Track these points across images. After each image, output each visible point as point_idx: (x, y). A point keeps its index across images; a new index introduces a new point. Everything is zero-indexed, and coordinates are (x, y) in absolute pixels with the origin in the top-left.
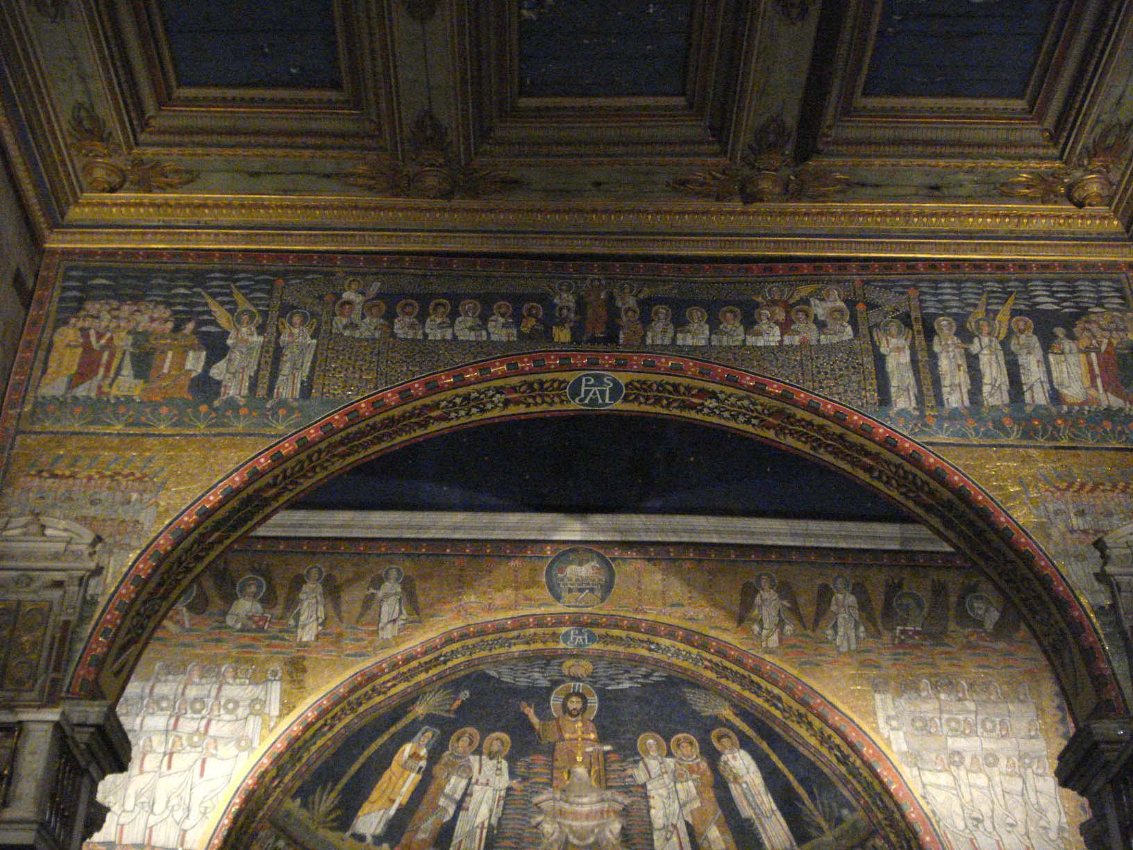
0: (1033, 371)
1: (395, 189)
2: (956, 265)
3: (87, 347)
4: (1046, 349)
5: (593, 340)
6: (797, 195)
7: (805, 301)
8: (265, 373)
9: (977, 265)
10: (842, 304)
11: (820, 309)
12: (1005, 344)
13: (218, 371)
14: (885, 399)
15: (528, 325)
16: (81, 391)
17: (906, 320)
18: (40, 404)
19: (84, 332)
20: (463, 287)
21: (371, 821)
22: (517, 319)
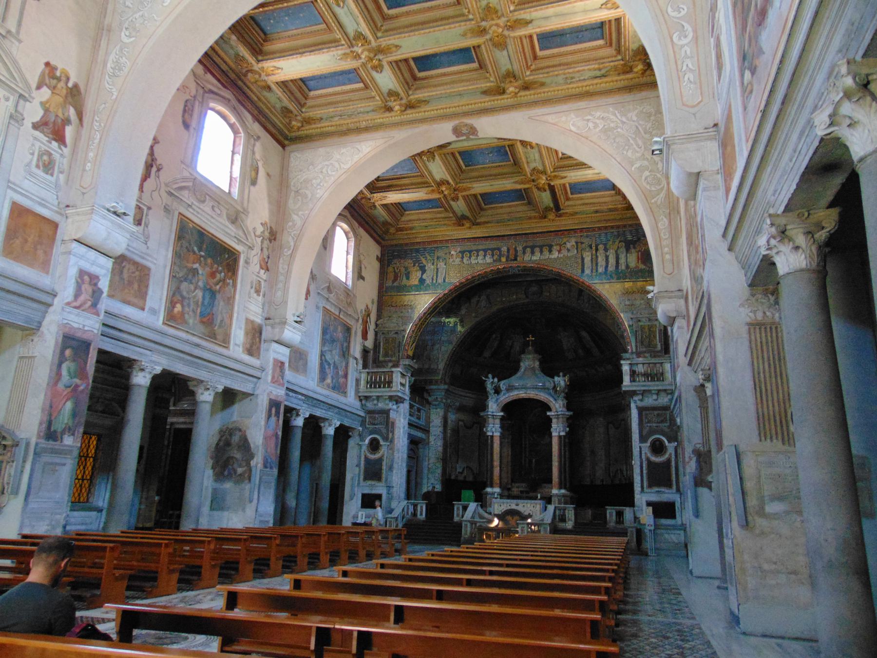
0: (622, 261)
1: (460, 225)
2: (606, 228)
3: (395, 271)
4: (627, 253)
5: (511, 260)
6: (560, 216)
7: (565, 243)
8: (435, 277)
9: (612, 227)
10: (574, 244)
11: (569, 245)
12: (616, 251)
13: (424, 277)
14: (583, 271)
15: (495, 257)
16: (395, 284)
17: (590, 246)
18: (387, 288)
19: (394, 268)
20: (480, 247)
21: (487, 354)
22: (493, 255)
